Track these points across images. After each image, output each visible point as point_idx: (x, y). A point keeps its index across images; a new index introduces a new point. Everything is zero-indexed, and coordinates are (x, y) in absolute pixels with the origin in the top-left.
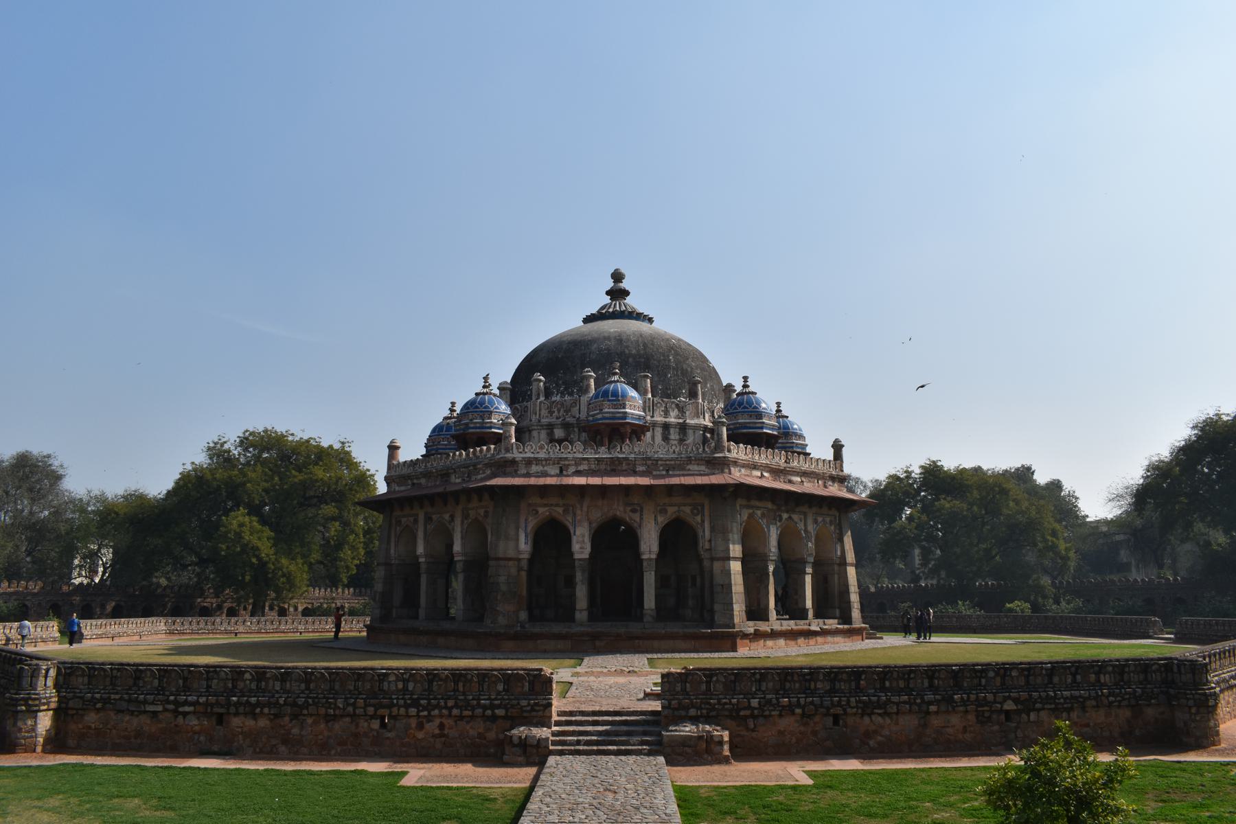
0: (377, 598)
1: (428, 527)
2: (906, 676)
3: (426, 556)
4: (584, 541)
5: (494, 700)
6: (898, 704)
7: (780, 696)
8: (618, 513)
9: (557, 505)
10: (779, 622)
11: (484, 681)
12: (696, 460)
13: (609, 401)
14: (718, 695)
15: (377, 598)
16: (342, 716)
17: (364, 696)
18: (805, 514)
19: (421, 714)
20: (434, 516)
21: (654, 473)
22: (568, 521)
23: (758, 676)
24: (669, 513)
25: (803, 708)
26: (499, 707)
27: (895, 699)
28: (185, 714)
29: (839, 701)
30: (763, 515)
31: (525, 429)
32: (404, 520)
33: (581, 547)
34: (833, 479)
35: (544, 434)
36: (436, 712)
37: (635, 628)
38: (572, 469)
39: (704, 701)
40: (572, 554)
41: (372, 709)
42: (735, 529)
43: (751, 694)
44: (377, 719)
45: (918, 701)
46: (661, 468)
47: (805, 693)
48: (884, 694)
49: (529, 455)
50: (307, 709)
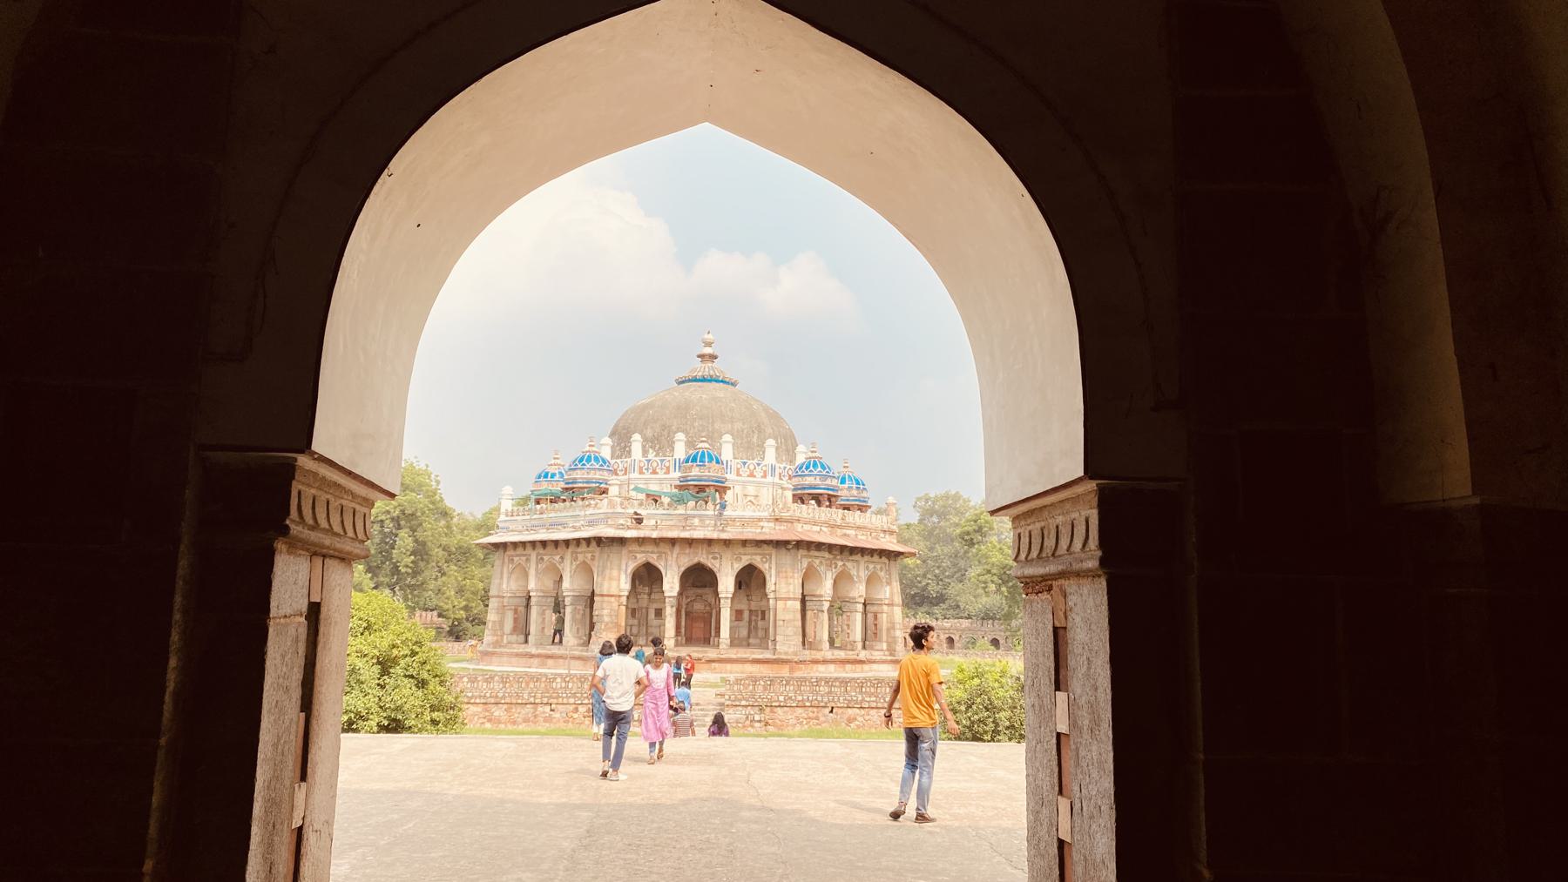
0: (490, 627)
1: (540, 566)
3: (537, 591)
4: (673, 582)
8: (702, 560)
9: (652, 553)
10: (830, 653)
13: (697, 465)
15: (490, 627)
20: (544, 557)
23: (784, 682)
24: (743, 561)
27: (868, 699)
29: (833, 699)
32: (516, 559)
33: (671, 584)
37: (711, 653)
41: (546, 699)
46: (738, 524)
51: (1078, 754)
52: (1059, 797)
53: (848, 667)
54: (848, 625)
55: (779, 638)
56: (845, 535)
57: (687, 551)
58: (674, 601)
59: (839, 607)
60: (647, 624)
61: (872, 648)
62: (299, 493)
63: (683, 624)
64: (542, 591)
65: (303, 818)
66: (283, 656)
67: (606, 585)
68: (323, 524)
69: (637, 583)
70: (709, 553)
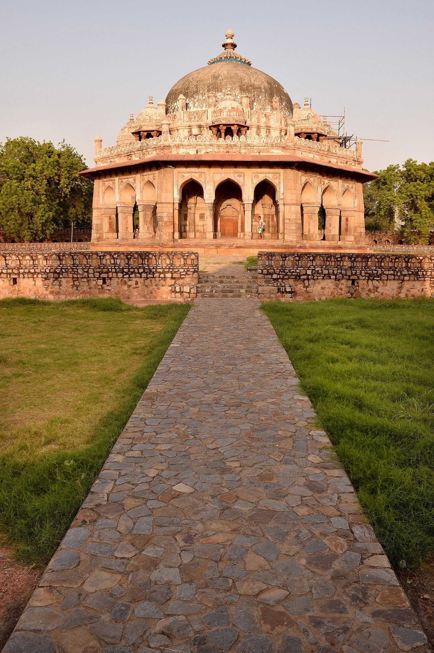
2: (393, 261)
5: (165, 269)
6: (388, 275)
7: (324, 269)
11: (159, 259)
12: (276, 146)
14: (289, 267)
15: (94, 228)
16: (82, 278)
17: (93, 268)
19: (125, 276)
23: (311, 258)
25: (336, 275)
26: (168, 272)
29: (356, 273)
31: (175, 129)
32: (106, 183)
36: (133, 275)
39: (282, 270)
42: (298, 188)
43: (307, 267)
44: (101, 279)
45: (399, 274)
47: (337, 268)
48: (380, 270)
49: (178, 142)
50: (62, 275)
56: (330, 162)
60: (194, 223)
67: (164, 195)
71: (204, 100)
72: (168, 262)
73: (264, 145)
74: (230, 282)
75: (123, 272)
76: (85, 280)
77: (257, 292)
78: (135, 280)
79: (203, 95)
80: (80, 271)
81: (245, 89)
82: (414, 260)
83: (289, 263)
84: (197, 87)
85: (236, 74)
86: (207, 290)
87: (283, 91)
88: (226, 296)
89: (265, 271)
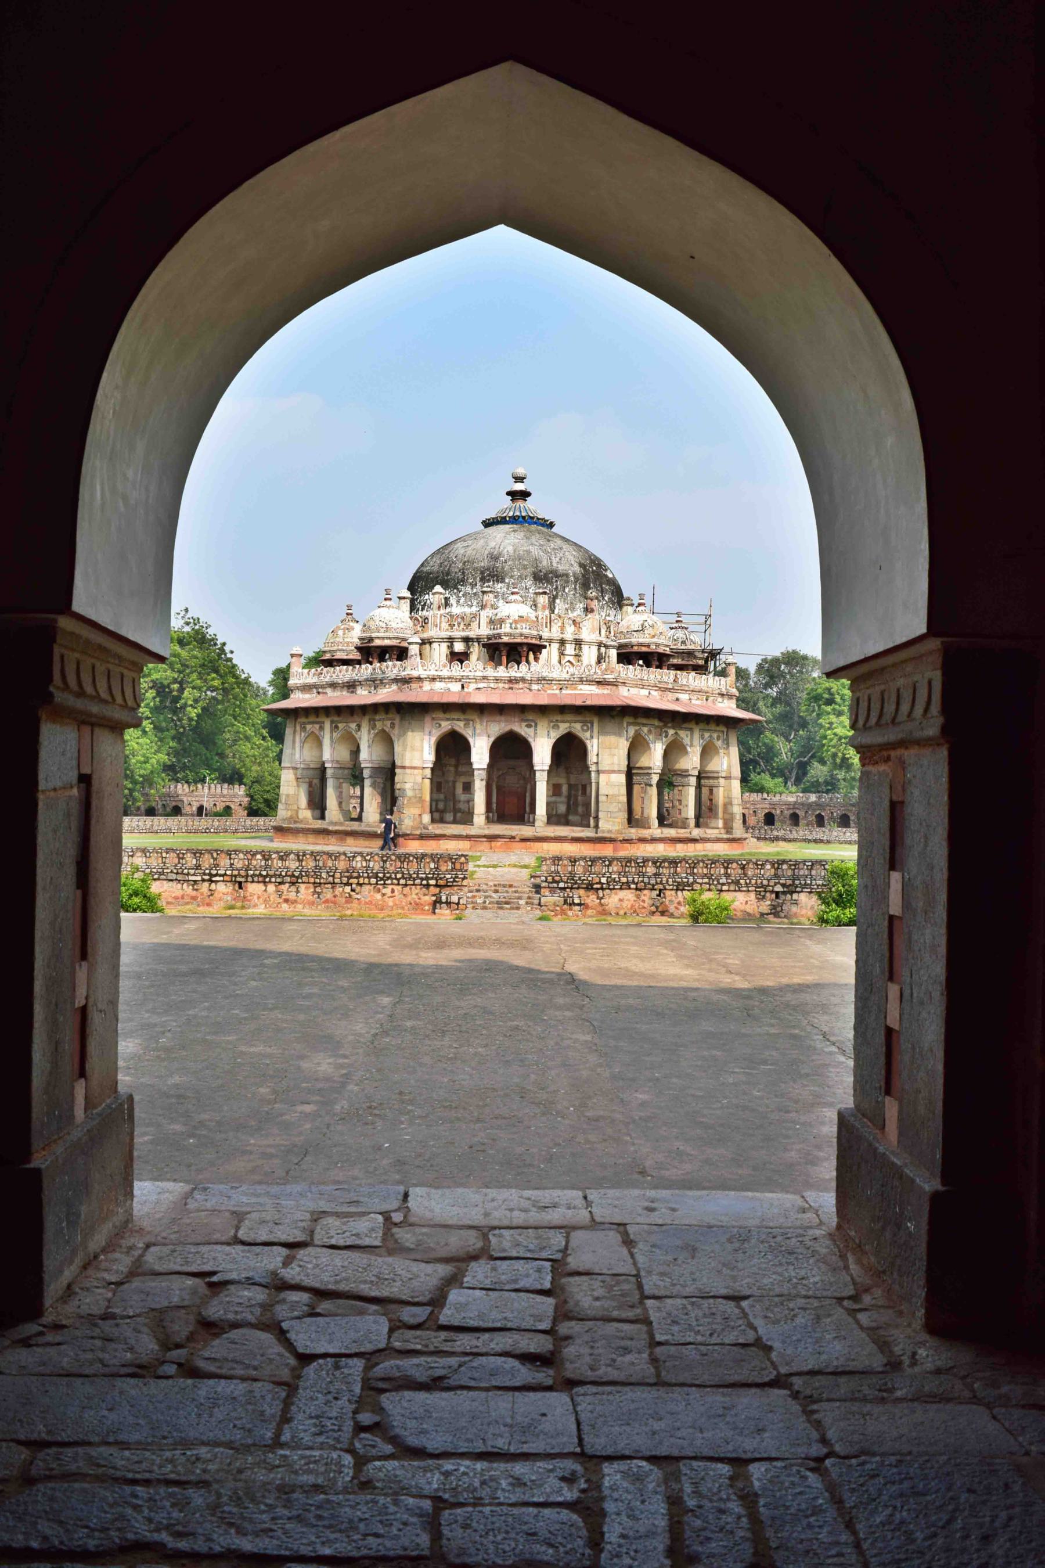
6: (701, 884)
9: (458, 720)
10: (659, 831)
18: (691, 730)
21: (549, 692)
22: (468, 733)
24: (561, 729)
25: (636, 884)
26: (432, 878)
27: (700, 881)
28: (216, 882)
30: (650, 731)
32: (309, 727)
34: (722, 695)
35: (444, 646)
36: (389, 882)
37: (526, 831)
38: (472, 687)
40: (471, 764)
42: (621, 745)
49: (433, 673)
51: (910, 940)
52: (889, 984)
53: (679, 846)
54: (680, 801)
55: (601, 815)
56: (677, 699)
57: (498, 718)
58: (484, 774)
59: (669, 780)
61: (707, 826)
62: (62, 657)
63: (494, 799)
64: (337, 762)
65: (87, 998)
66: (55, 831)
67: (408, 755)
68: (89, 689)
69: (442, 754)
70: (523, 720)
71: (475, 594)
72: (432, 865)
73: (567, 676)
74: (507, 892)
75: (376, 877)
76: (329, 886)
77: (539, 904)
78: (391, 887)
79: (473, 586)
80: (324, 875)
81: (542, 577)
82: (734, 865)
83: (579, 869)
84: (463, 573)
85: (529, 552)
86: (480, 901)
87: (606, 576)
88: (501, 908)
89: (550, 879)
